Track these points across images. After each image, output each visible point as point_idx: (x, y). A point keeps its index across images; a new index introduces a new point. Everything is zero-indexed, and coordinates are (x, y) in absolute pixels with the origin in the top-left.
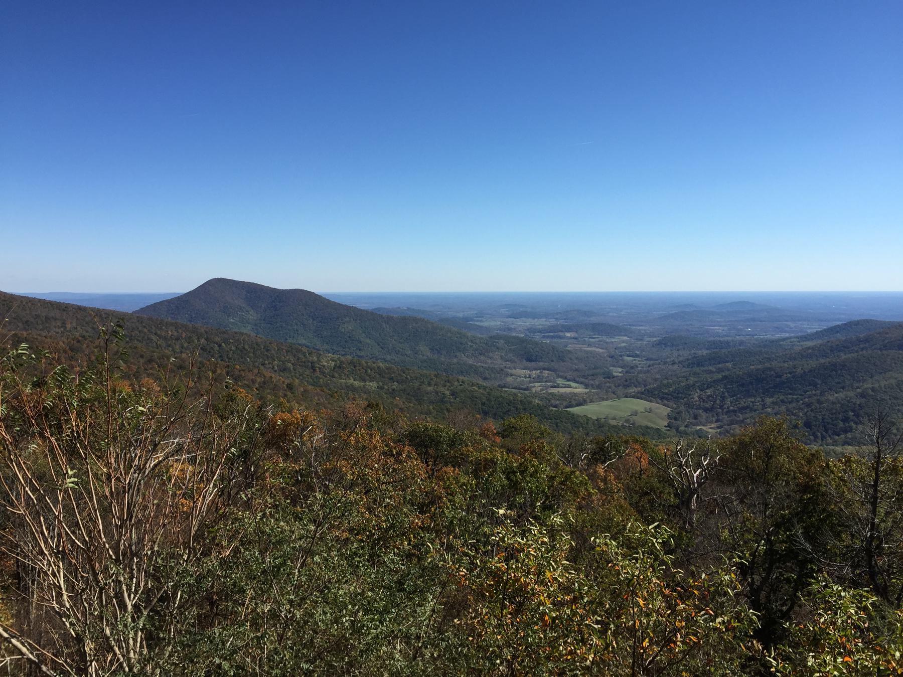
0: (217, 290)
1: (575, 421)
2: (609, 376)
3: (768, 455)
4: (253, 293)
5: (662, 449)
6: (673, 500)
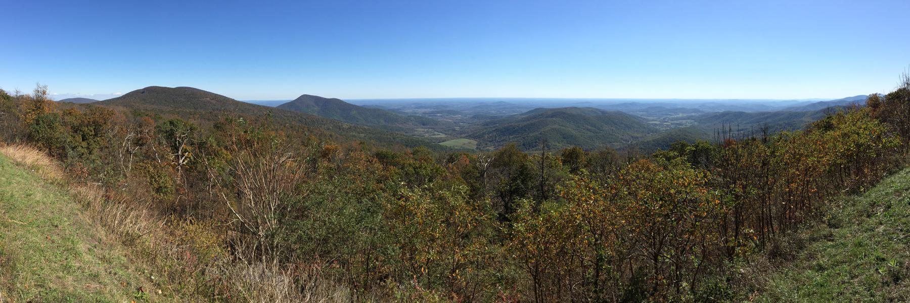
0: (304, 98)
1: (442, 148)
2: (454, 130)
3: (510, 156)
4: (317, 100)
5: (474, 157)
6: (478, 175)
